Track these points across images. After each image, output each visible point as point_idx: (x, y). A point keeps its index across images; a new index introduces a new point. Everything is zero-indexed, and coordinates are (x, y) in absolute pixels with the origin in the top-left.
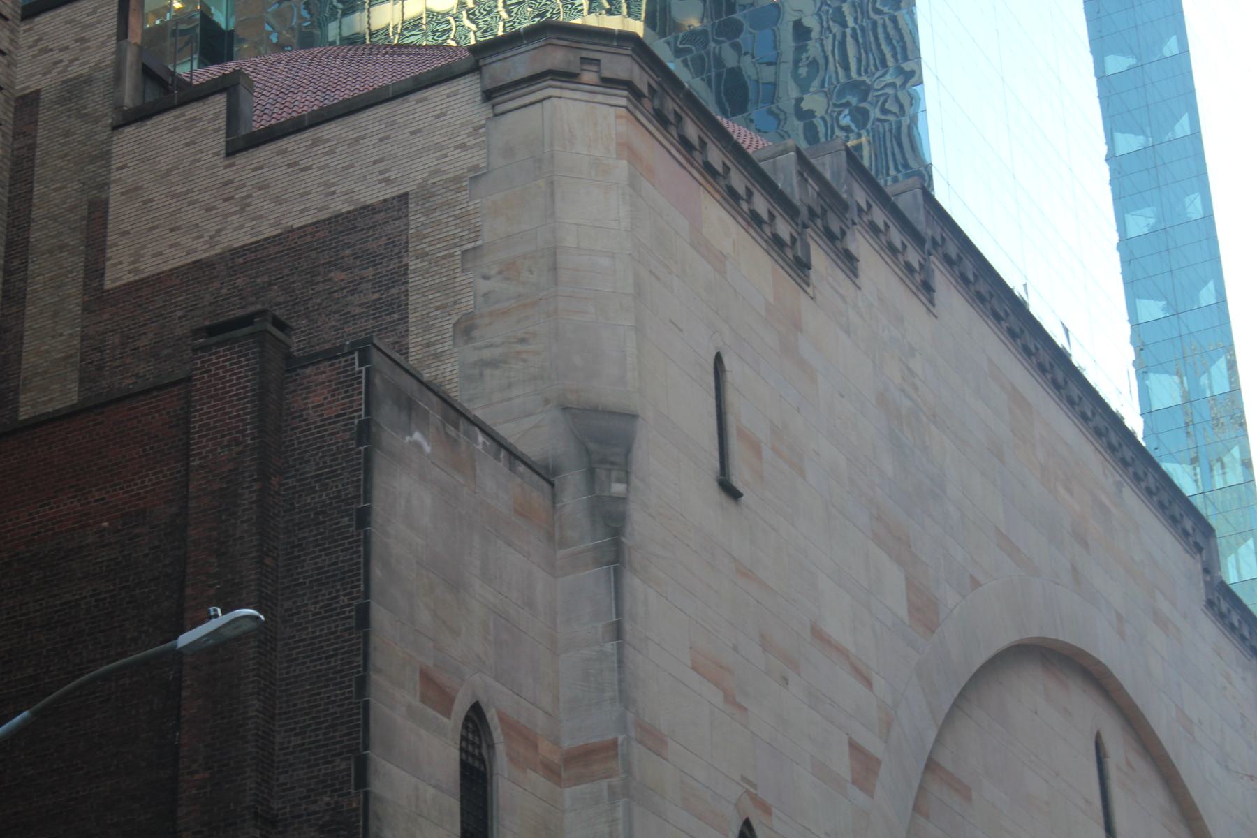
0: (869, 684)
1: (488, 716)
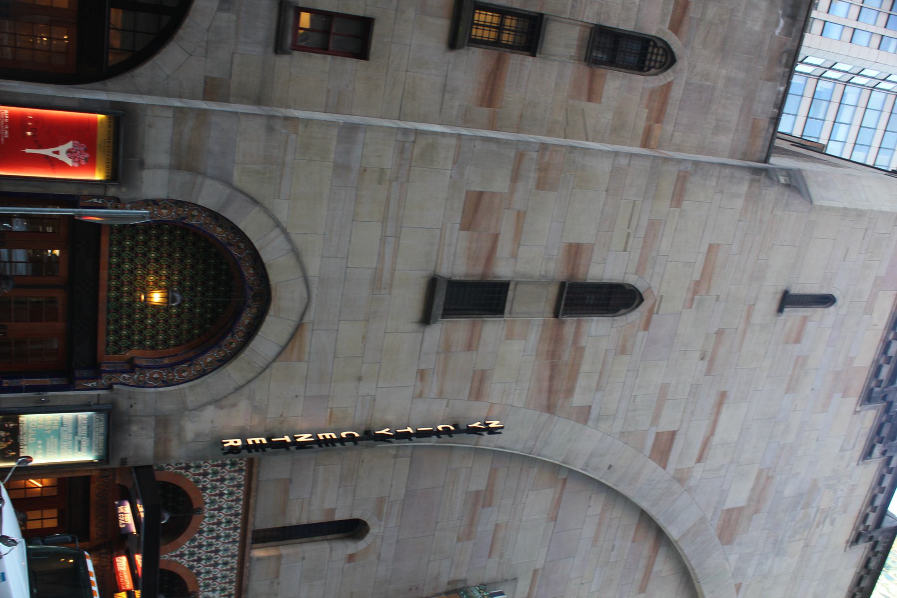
0: (699, 460)
1: (669, 71)
